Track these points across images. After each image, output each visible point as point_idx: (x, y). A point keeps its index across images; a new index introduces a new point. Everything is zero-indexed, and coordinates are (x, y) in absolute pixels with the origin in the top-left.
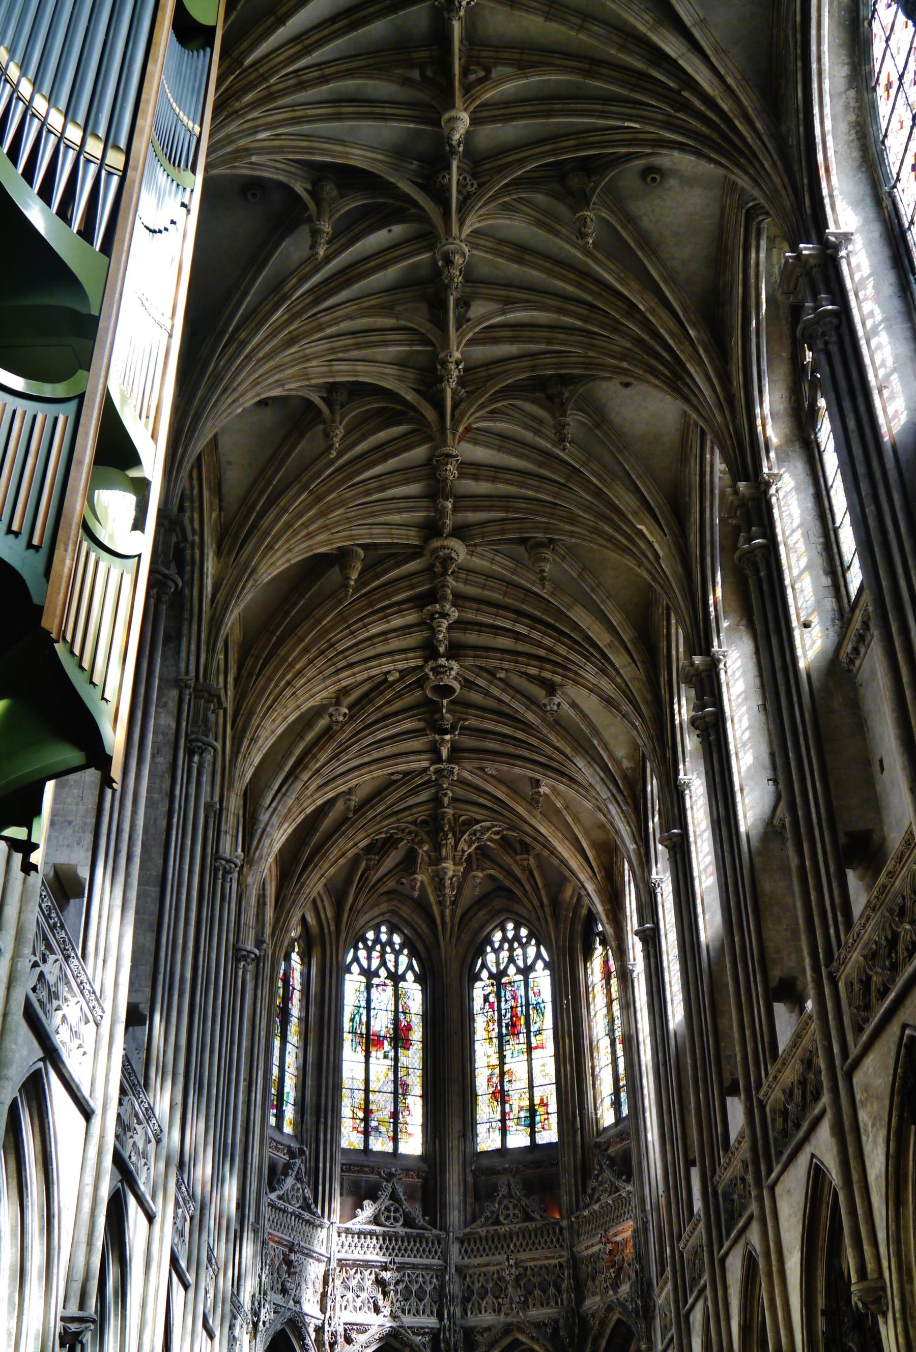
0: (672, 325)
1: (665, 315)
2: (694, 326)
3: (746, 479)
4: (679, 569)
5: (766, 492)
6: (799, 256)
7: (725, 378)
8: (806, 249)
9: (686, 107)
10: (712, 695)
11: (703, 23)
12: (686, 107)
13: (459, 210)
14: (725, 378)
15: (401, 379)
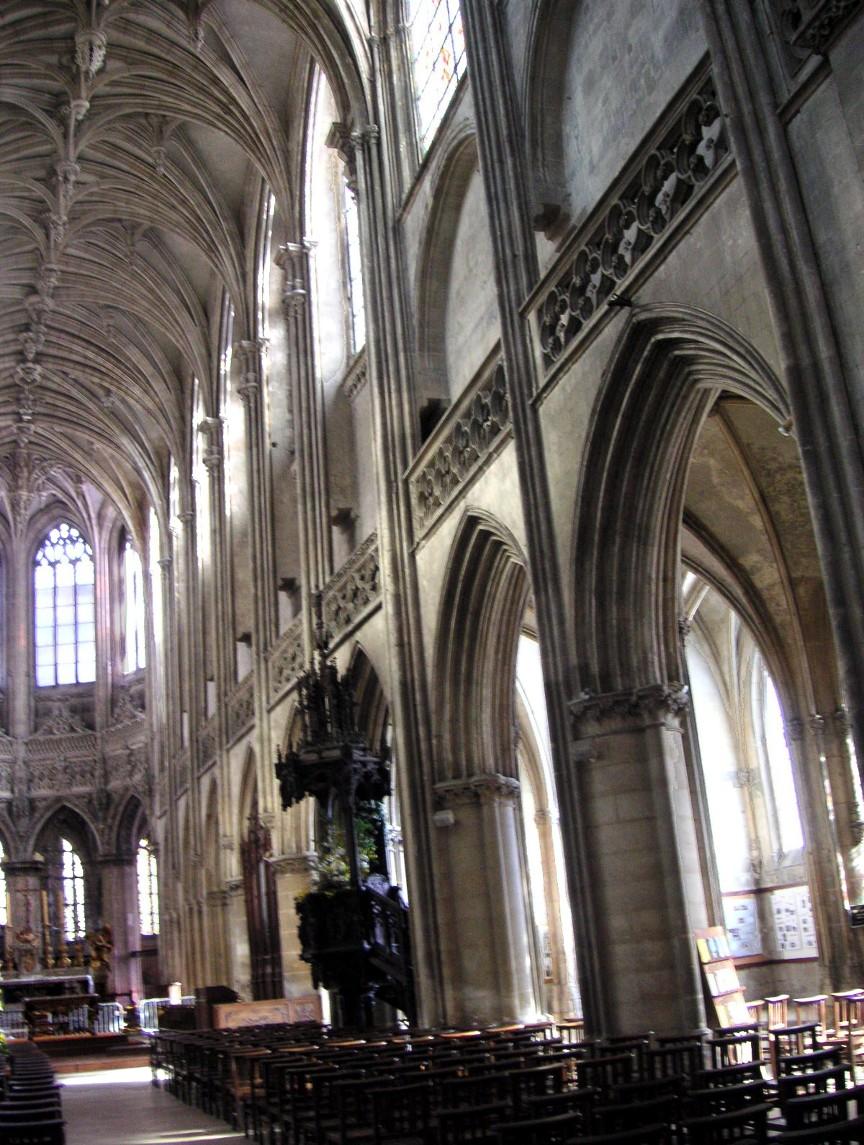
0: (212, 216)
1: (207, 208)
2: (225, 219)
3: (249, 339)
4: (204, 351)
5: (259, 350)
6: (287, 250)
7: (242, 257)
8: (292, 247)
9: (230, 113)
10: (218, 445)
11: (247, 65)
12: (230, 113)
13: (75, 135)
14: (242, 257)
15: (19, 208)
